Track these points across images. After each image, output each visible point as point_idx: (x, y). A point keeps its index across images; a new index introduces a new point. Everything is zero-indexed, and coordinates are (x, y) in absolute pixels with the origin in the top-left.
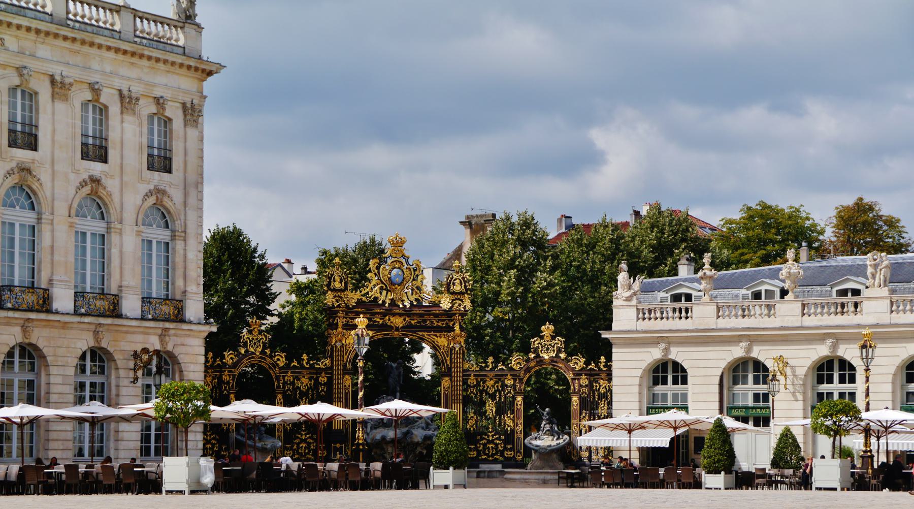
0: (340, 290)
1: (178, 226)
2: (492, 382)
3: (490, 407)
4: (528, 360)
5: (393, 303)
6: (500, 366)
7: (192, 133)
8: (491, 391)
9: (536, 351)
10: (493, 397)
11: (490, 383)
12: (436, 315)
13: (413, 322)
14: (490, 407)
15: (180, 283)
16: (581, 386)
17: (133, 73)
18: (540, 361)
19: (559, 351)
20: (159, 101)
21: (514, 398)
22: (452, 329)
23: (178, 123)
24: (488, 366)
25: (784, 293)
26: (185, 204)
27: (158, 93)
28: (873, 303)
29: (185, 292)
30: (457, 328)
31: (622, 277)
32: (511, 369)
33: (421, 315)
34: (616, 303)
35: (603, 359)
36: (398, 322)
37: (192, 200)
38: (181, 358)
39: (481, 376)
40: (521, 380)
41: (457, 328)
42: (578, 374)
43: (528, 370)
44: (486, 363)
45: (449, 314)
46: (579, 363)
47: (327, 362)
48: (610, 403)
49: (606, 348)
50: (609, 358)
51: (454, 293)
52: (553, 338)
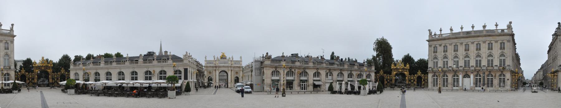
1: (10, 57)
3: (56, 80)
5: (42, 65)
7: (12, 45)
14: (56, 80)
15: (10, 64)
17: (2, 37)
20: (6, 41)
21: (58, 78)
23: (10, 43)
26: (11, 54)
27: (6, 40)
29: (11, 65)
36: (43, 68)
37: (12, 53)
38: (10, 74)
39: (54, 75)
43: (60, 74)
45: (50, 67)
47: (34, 74)
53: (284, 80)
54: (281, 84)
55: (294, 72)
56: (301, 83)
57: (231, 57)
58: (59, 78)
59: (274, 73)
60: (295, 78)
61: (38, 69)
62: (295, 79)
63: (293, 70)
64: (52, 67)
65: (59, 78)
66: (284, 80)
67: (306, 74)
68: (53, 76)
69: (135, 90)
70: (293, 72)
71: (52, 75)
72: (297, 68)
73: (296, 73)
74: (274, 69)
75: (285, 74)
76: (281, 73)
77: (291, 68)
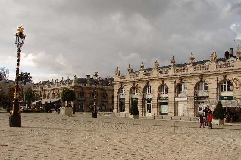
69: (13, 114)
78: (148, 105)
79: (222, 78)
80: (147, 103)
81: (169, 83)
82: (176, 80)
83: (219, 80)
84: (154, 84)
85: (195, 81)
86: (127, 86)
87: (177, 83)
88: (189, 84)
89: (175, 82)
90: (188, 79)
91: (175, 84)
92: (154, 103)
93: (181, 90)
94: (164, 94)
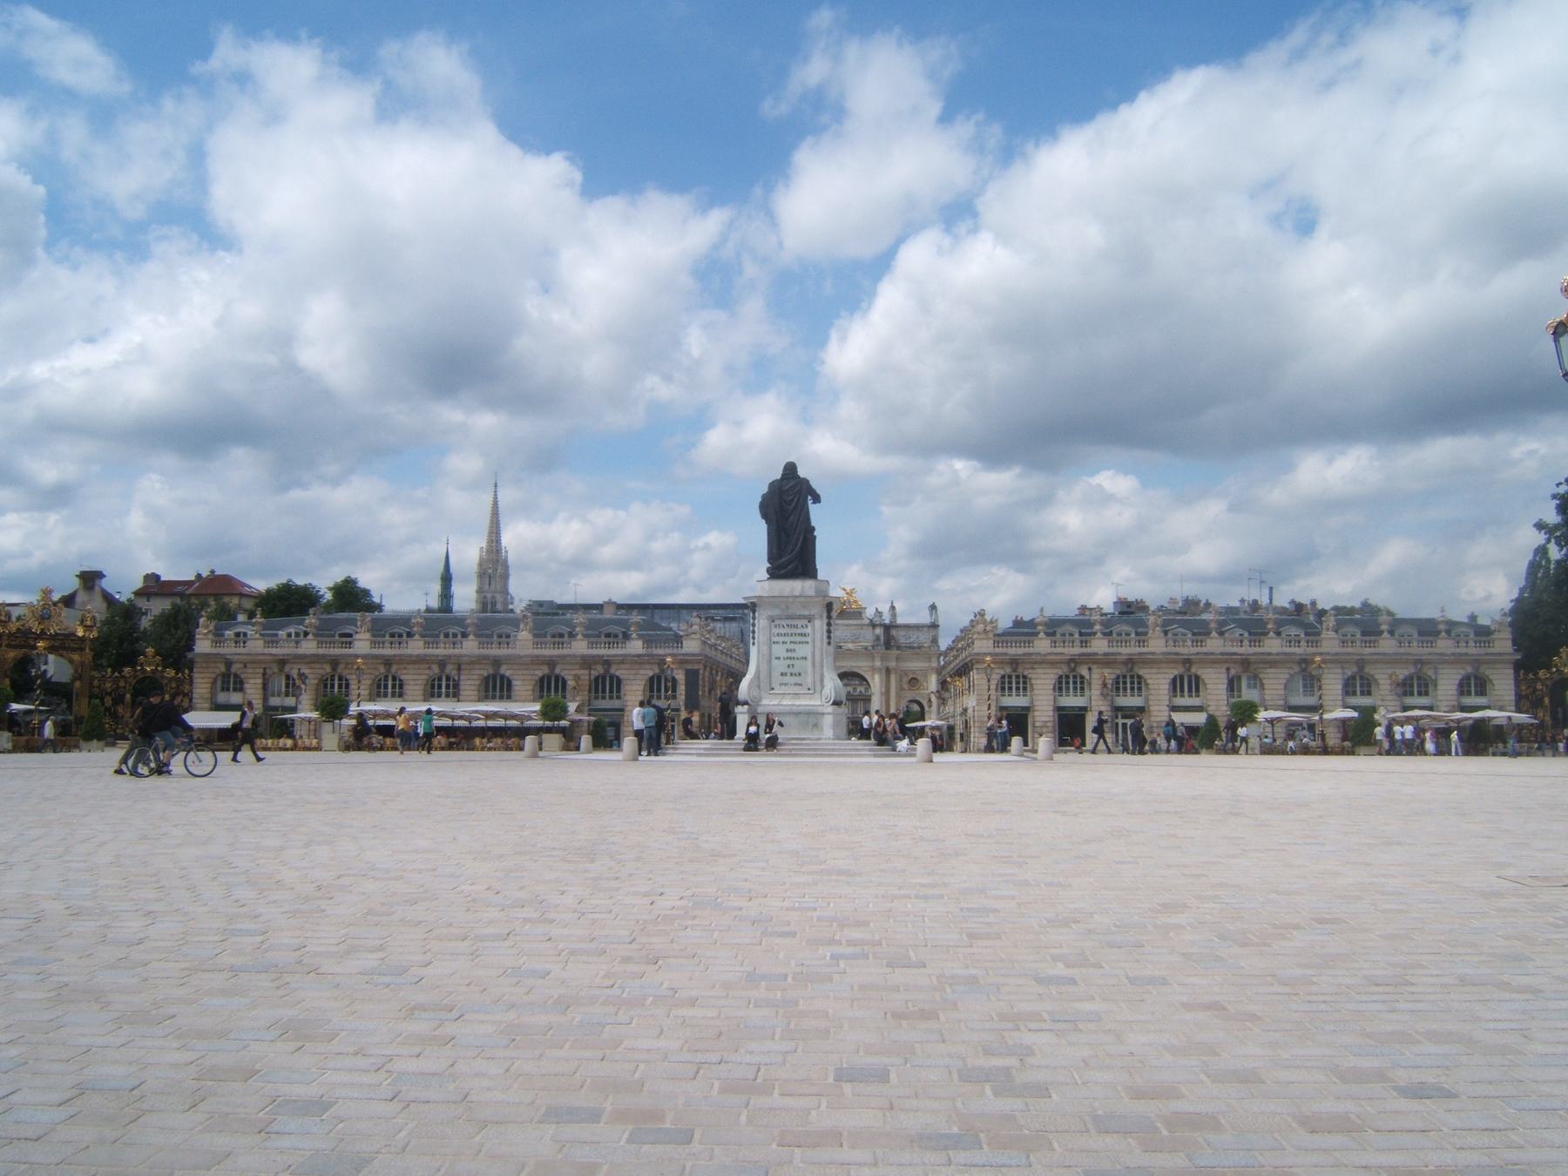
0: (5, 622)
2: (110, 685)
4: (136, 671)
6: (116, 674)
8: (109, 690)
9: (141, 665)
10: (110, 694)
11: (108, 685)
12: (73, 640)
13: (56, 644)
16: (171, 688)
18: (144, 671)
19: (158, 665)
21: (124, 695)
22: (82, 650)
24: (107, 674)
25: (306, 634)
28: (361, 642)
30: (87, 651)
31: (202, 620)
32: (124, 676)
33: (62, 640)
34: (197, 636)
35: (187, 671)
40: (130, 684)
41: (87, 651)
42: (171, 679)
44: (106, 672)
45: (82, 639)
46: (170, 673)
48: (191, 700)
49: (191, 665)
50: (191, 670)
51: (86, 626)
52: (154, 657)
53: (990, 705)
54: (1034, 722)
55: (1087, 677)
56: (1120, 721)
57: (885, 609)
58: (128, 696)
59: (1067, 683)
60: (1043, 702)
61: (15, 647)
62: (1093, 703)
63: (1084, 672)
64: (91, 640)
65: (128, 696)
66: (990, 705)
67: (1138, 684)
68: (96, 683)
70: (1082, 677)
71: (93, 678)
72: (1098, 663)
73: (1093, 682)
74: (1008, 670)
75: (993, 687)
76: (1033, 682)
77: (1073, 662)
78: (1124, 725)
79: (1355, 669)
80: (1120, 721)
81: (1208, 670)
82: (1232, 665)
83: (1349, 673)
84: (1155, 671)
85: (1287, 671)
86: (1039, 671)
87: (1233, 672)
88: (1271, 676)
89: (1228, 669)
90: (1267, 666)
91: (1228, 673)
92: (1159, 719)
93: (1240, 690)
94: (1182, 696)
